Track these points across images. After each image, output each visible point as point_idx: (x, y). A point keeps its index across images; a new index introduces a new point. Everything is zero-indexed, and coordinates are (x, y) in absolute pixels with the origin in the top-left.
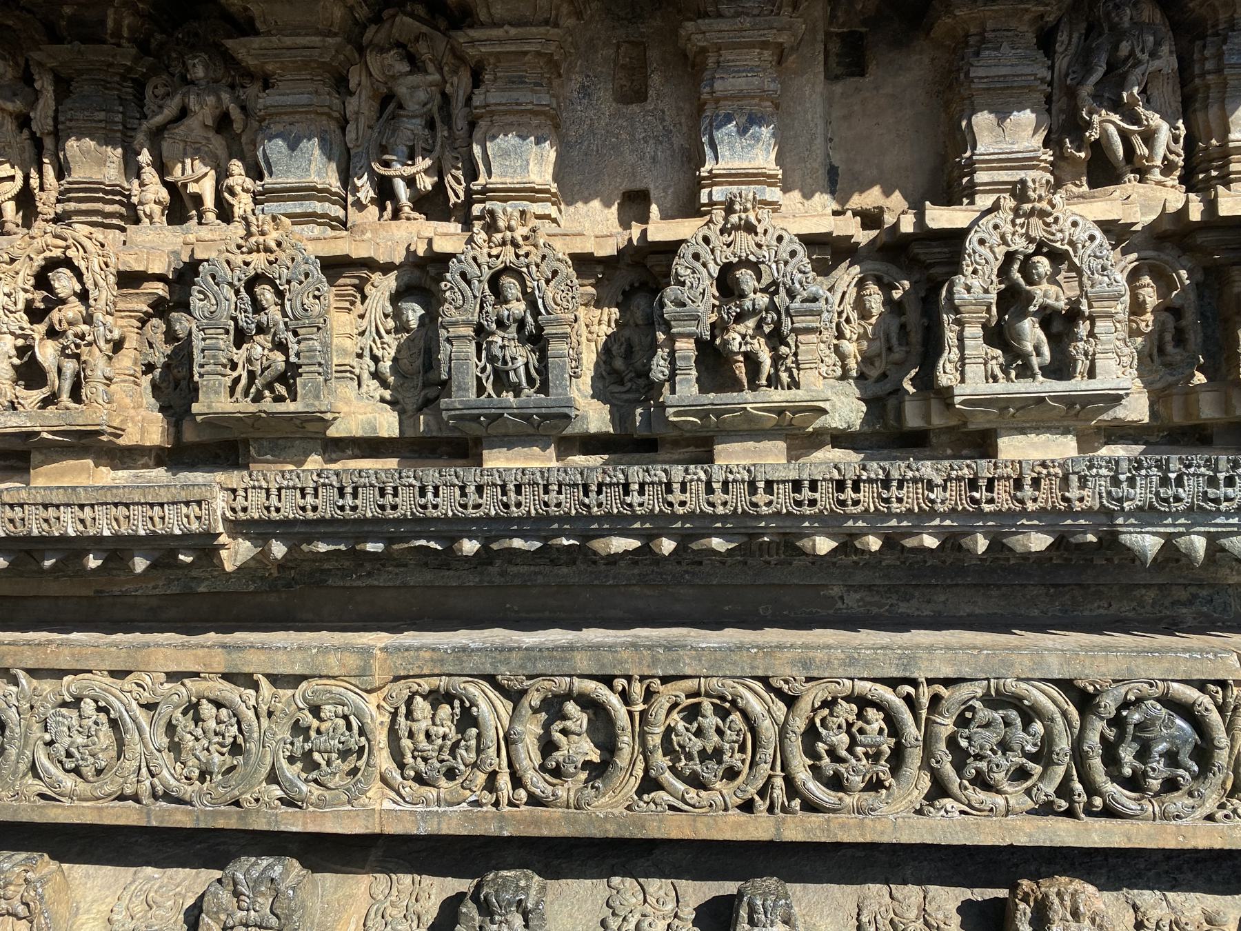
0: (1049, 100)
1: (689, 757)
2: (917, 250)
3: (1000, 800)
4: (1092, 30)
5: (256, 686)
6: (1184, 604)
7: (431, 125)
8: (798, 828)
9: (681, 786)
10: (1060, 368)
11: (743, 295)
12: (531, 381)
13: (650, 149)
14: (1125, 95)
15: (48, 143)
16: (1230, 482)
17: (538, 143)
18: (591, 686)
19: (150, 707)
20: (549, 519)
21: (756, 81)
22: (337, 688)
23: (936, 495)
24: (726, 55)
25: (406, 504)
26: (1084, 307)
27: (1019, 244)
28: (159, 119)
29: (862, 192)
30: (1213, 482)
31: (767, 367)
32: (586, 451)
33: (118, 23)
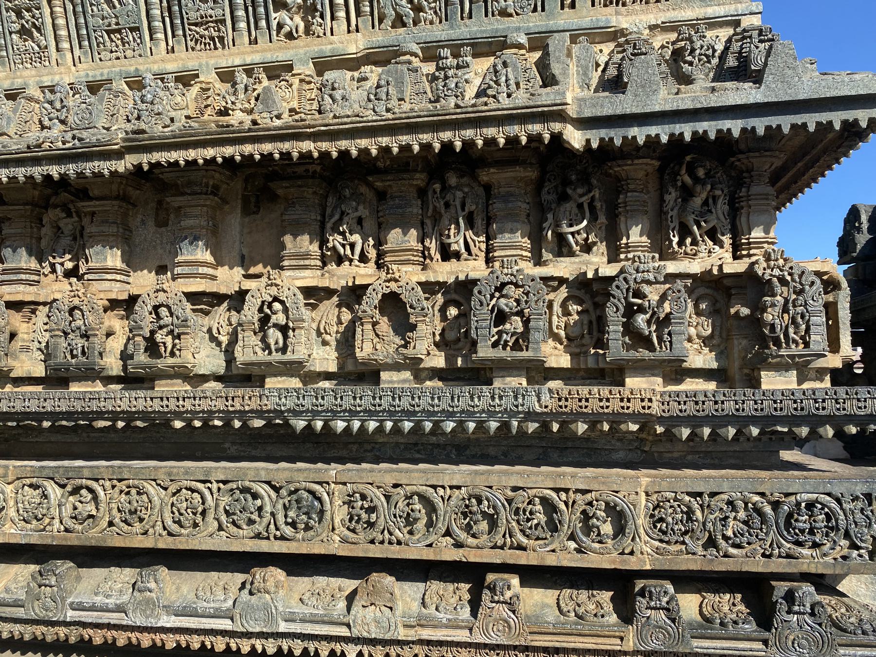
3: (241, 531)
4: (340, 198)
6: (369, 452)
7: (75, 239)
12: (83, 353)
13: (168, 247)
14: (341, 229)
17: (111, 248)
18: (90, 483)
21: (197, 221)
24: (188, 210)
26: (291, 324)
29: (254, 266)
32: (118, 383)
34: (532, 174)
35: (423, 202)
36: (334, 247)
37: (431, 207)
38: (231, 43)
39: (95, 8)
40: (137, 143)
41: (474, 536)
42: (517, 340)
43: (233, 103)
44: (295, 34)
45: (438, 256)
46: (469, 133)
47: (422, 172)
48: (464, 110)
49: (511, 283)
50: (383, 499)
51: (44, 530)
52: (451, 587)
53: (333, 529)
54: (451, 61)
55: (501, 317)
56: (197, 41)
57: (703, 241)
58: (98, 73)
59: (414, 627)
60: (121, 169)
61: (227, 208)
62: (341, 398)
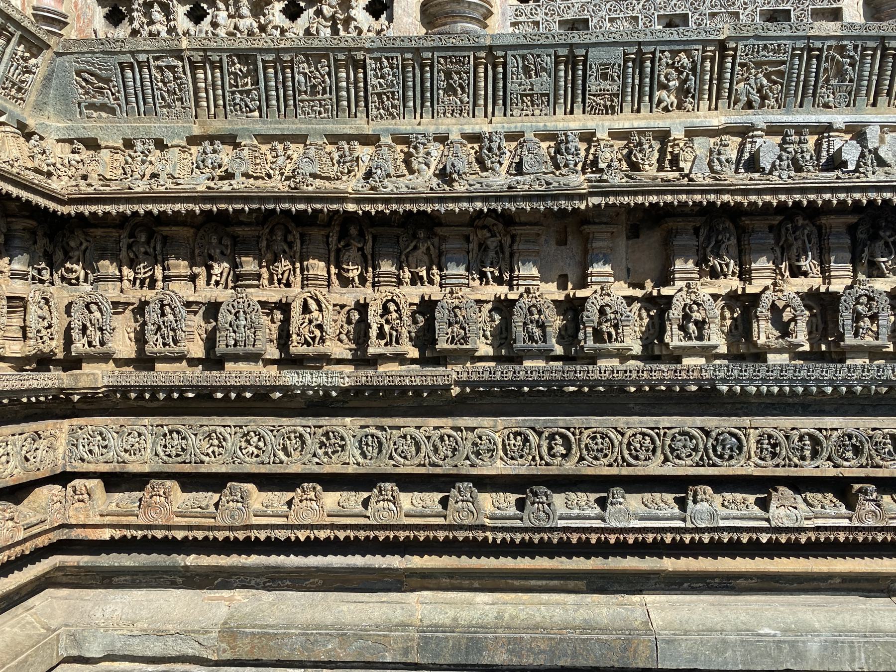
0: (697, 250)
1: (593, 451)
2: (658, 300)
4: (711, 229)
5: (462, 431)
7: (497, 253)
8: (625, 471)
10: (700, 338)
11: (607, 315)
15: (369, 257)
16: (746, 371)
18: (563, 430)
19: (428, 438)
20: (553, 381)
22: (487, 431)
23: (665, 374)
25: (509, 376)
27: (688, 301)
30: (741, 371)
31: (614, 337)
37: (783, 239)
39: (514, 77)
41: (847, 460)
45: (787, 274)
46: (842, 196)
49: (866, 295)
52: (820, 496)
53: (750, 458)
54: (795, 138)
56: (593, 107)
58: (513, 125)
59: (810, 519)
60: (583, 207)
62: (759, 371)
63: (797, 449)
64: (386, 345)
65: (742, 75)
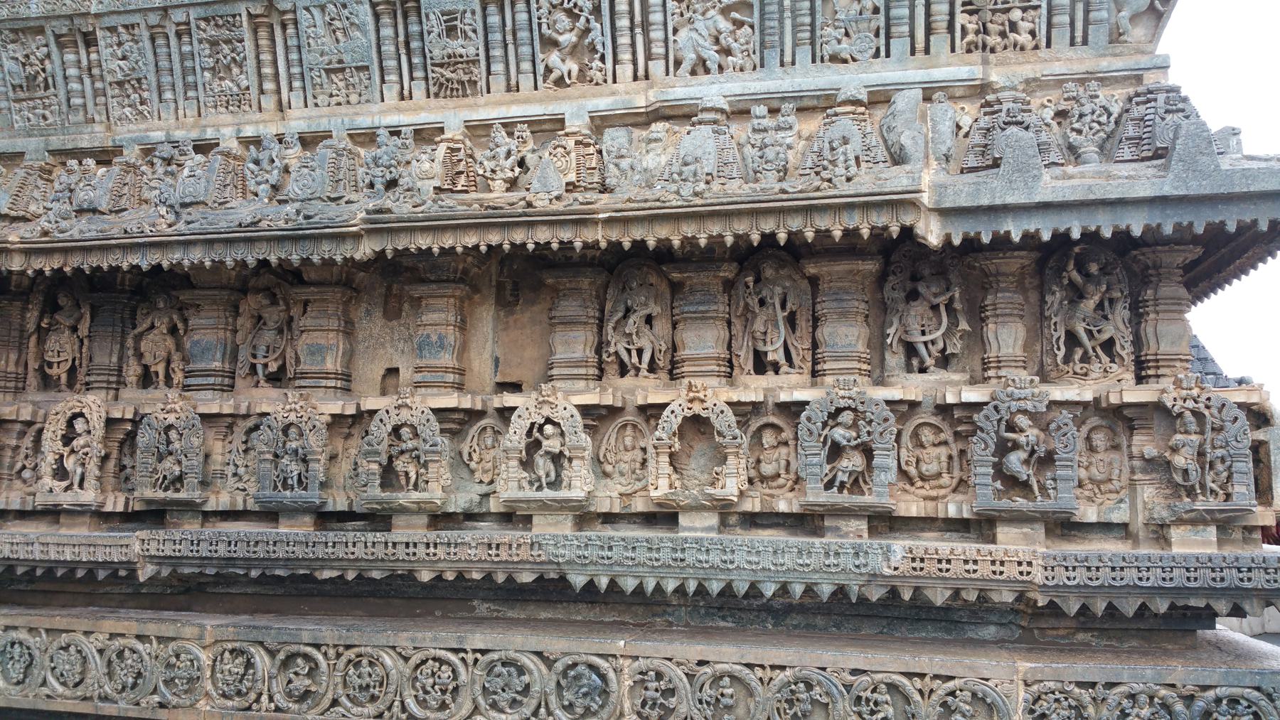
9: (349, 705)
12: (300, 481)
13: (401, 345)
18: (309, 649)
21: (443, 316)
26: (567, 453)
28: (139, 329)
33: (123, 279)
34: (871, 266)
35: (730, 296)
36: (616, 353)
37: (742, 304)
38: (485, 90)
40: (378, 225)
42: (856, 480)
43: (493, 171)
44: (568, 81)
47: (732, 260)
48: (790, 196)
49: (849, 408)
50: (685, 679)
51: (249, 708)
55: (836, 451)
57: (1097, 356)
61: (477, 297)
63: (708, 703)
64: (67, 489)
65: (682, 15)
